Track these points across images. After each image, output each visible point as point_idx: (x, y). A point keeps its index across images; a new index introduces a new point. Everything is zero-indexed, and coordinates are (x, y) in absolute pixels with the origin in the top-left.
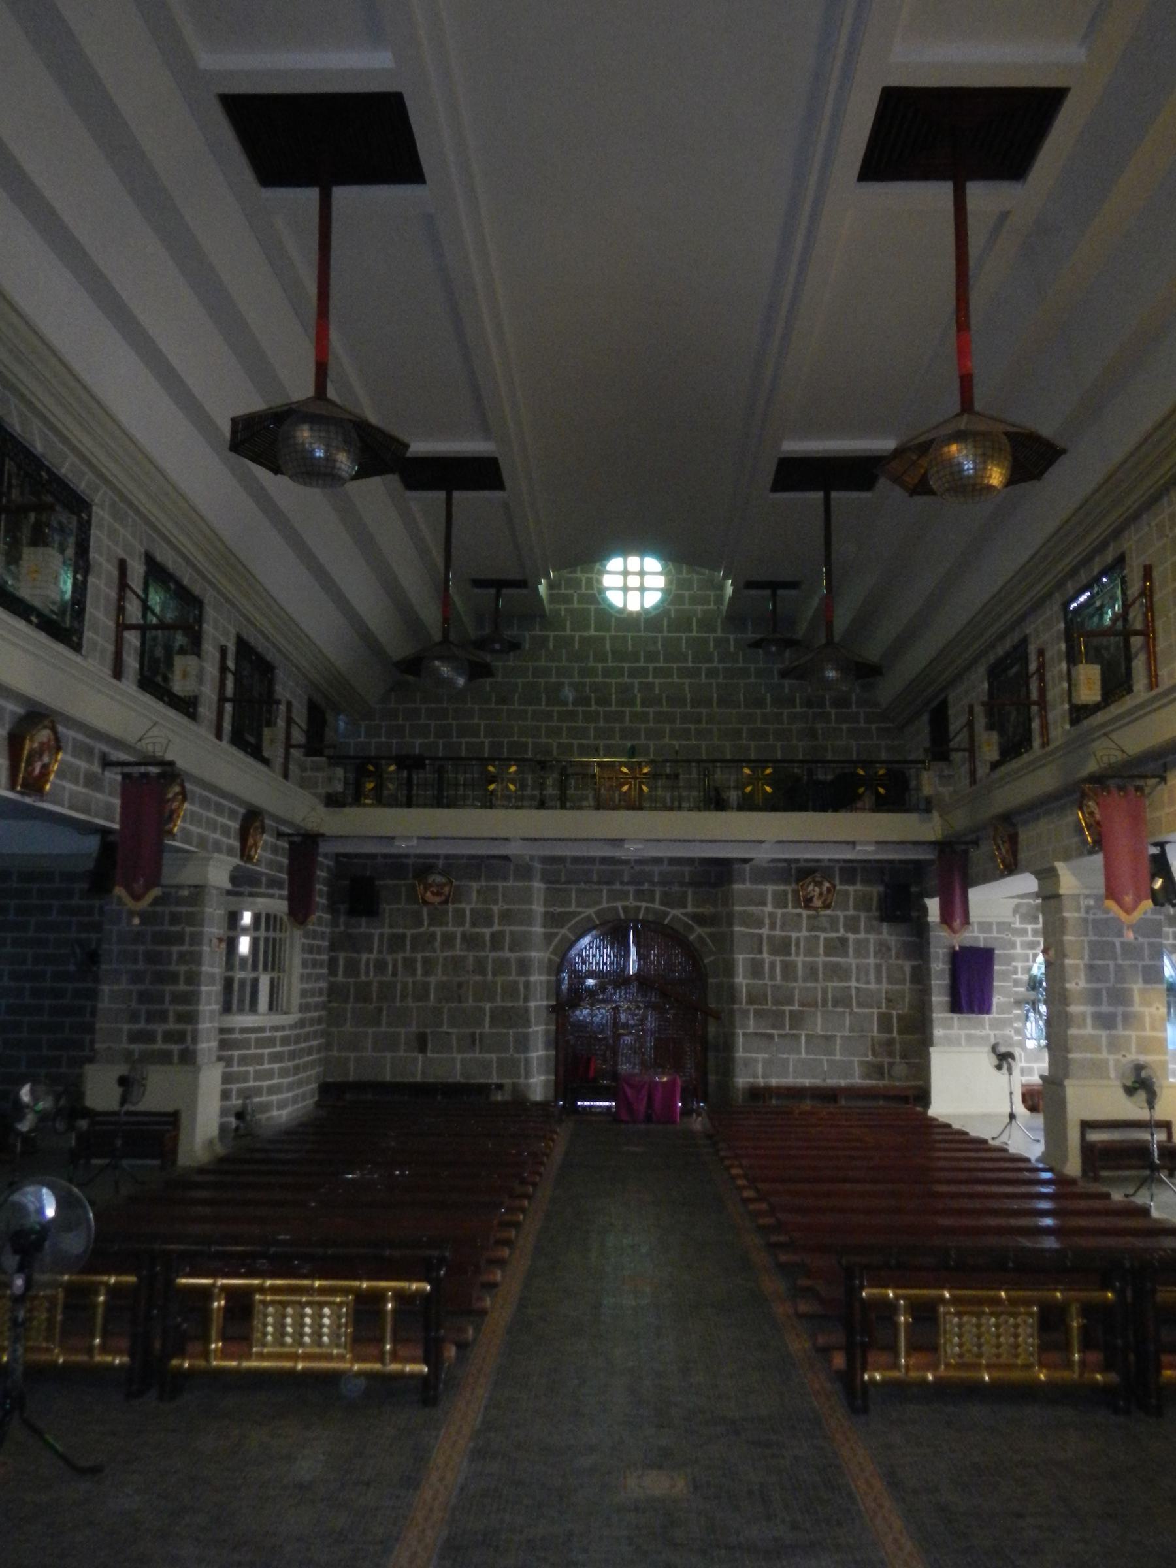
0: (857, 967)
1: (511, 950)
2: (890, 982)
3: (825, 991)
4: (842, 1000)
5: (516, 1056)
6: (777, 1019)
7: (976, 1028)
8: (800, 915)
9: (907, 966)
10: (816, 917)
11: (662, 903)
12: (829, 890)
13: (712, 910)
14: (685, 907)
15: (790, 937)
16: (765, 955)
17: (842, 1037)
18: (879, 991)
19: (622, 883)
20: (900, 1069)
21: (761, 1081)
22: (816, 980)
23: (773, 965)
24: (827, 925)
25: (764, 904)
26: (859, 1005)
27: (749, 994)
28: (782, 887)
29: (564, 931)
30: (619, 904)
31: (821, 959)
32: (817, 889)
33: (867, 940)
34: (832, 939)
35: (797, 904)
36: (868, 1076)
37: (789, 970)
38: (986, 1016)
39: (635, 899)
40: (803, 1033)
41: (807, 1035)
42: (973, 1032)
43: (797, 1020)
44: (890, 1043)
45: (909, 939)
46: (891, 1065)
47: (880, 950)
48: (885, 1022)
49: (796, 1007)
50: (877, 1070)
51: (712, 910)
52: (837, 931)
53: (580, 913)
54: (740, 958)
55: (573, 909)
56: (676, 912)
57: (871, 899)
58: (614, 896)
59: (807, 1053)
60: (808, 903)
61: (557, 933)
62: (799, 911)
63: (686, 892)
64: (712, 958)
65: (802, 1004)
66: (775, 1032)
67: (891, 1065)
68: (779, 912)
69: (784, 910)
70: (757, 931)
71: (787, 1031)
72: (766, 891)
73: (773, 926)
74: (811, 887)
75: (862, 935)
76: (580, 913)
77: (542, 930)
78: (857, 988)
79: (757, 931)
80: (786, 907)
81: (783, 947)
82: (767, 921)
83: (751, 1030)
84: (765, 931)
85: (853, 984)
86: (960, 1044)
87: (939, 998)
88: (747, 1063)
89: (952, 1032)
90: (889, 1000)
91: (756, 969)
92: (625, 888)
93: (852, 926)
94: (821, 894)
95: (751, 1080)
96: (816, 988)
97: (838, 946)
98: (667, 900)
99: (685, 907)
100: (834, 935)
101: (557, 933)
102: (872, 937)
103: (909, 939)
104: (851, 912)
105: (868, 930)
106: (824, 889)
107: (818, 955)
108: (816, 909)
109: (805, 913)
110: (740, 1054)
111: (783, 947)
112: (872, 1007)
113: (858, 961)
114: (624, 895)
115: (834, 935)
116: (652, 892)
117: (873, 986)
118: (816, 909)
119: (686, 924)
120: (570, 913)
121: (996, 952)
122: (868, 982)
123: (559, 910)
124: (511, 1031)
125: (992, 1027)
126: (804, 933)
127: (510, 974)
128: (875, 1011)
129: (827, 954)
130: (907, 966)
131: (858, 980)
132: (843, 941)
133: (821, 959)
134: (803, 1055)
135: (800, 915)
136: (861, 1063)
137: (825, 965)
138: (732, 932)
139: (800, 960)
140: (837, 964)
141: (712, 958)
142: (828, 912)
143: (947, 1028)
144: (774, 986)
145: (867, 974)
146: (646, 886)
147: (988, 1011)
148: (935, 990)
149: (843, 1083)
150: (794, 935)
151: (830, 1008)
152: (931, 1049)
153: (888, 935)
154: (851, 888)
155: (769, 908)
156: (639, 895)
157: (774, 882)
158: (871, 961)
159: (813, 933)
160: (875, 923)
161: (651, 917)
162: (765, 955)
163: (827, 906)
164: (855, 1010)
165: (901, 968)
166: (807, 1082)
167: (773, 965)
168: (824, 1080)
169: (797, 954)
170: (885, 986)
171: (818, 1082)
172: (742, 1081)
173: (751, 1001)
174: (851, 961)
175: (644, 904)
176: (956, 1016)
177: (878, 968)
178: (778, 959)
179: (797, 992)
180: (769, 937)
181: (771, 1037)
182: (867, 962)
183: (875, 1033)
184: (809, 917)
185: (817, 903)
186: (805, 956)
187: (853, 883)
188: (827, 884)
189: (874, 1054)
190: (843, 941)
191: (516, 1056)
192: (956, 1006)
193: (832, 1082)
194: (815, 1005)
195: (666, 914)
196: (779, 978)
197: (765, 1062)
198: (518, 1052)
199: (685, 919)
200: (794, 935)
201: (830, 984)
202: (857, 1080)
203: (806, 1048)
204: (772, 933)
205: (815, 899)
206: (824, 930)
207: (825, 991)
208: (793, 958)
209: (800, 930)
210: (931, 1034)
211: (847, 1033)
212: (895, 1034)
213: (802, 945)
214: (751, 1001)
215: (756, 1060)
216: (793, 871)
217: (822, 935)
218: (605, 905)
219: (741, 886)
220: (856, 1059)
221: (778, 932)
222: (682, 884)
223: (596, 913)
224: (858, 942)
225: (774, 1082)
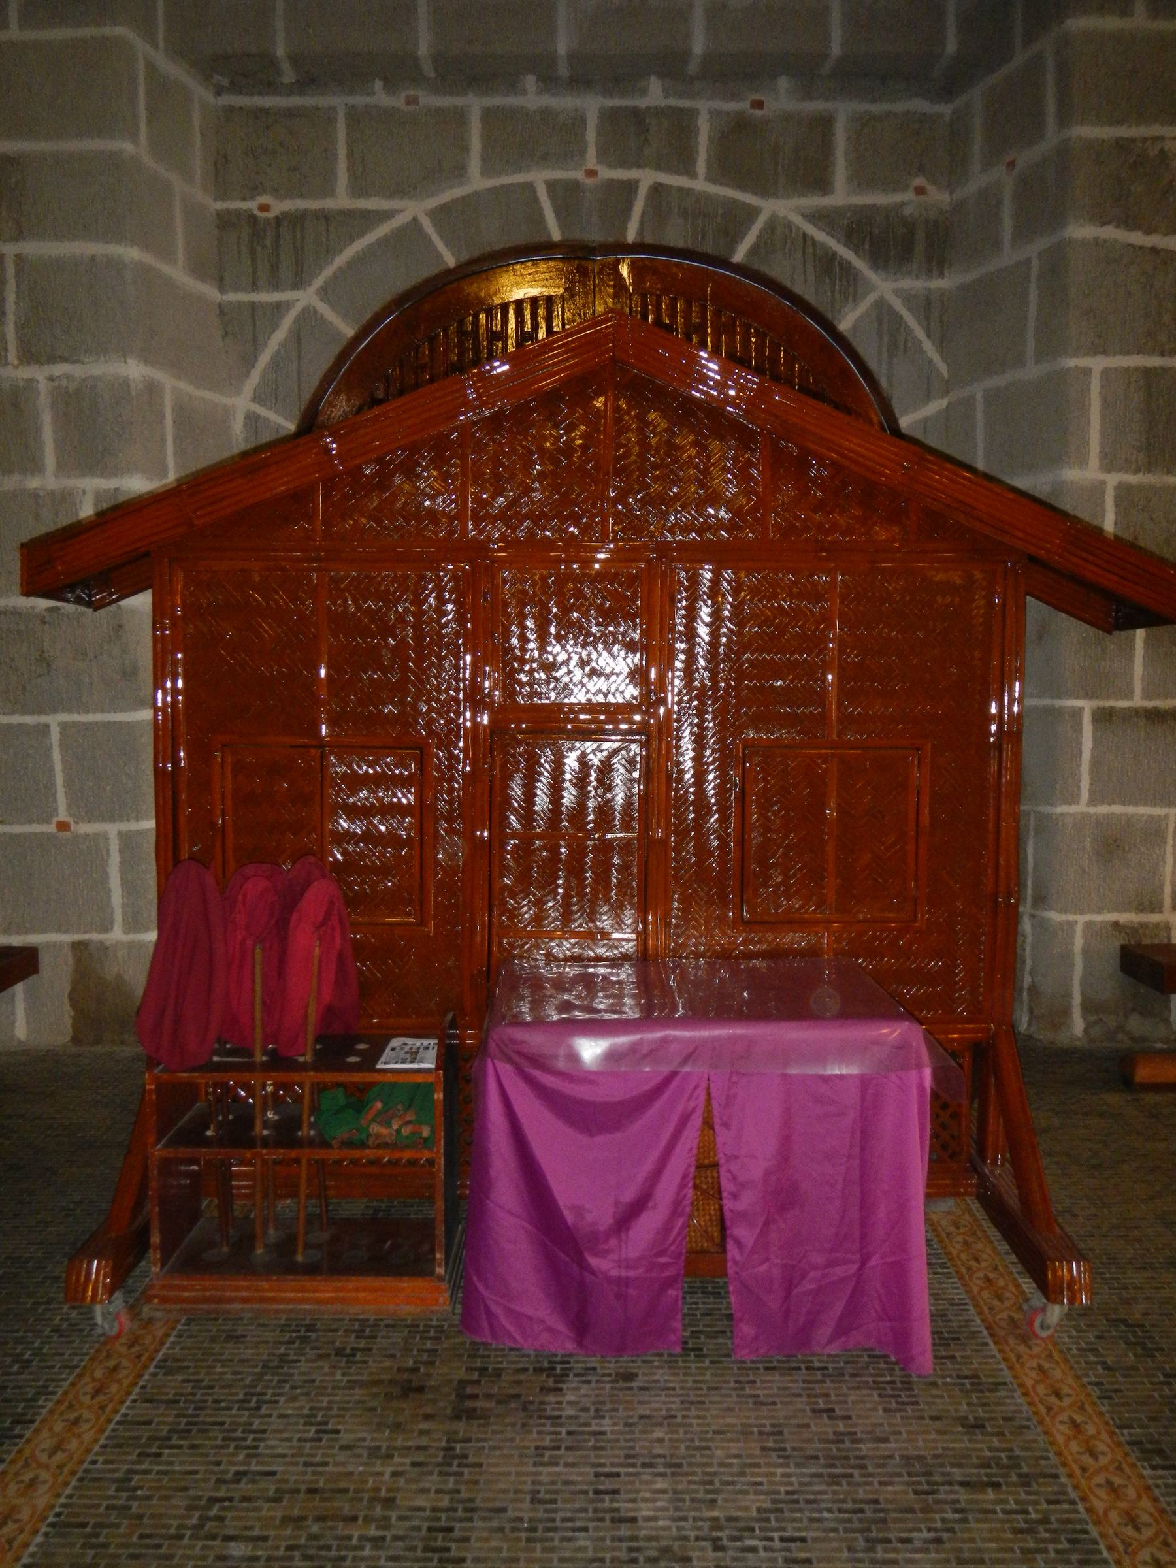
1: (29, 356)
5: (85, 828)
11: (727, 167)
13: (939, 197)
14: (822, 185)
19: (549, 82)
29: (305, 298)
30: (539, 177)
39: (603, 154)
51: (939, 197)
53: (370, 219)
55: (341, 200)
56: (786, 208)
58: (515, 139)
61: (279, 309)
63: (825, 123)
64: (936, 406)
76: (370, 219)
77: (210, 292)
83: (1138, 701)
92: (565, 103)
98: (745, 154)
99: (822, 185)
101: (279, 309)
114: (563, 137)
116: (681, 125)
119: (828, 264)
120: (325, 217)
123: (280, 206)
124: (54, 721)
127: (34, 465)
141: (936, 406)
146: (655, 94)
156: (628, 134)
161: (675, 235)
175: (646, 178)
191: (85, 828)
195: (736, 220)
198: (91, 815)
199: (821, 236)
218: (477, 181)
222: (806, 71)
223: (440, 215)
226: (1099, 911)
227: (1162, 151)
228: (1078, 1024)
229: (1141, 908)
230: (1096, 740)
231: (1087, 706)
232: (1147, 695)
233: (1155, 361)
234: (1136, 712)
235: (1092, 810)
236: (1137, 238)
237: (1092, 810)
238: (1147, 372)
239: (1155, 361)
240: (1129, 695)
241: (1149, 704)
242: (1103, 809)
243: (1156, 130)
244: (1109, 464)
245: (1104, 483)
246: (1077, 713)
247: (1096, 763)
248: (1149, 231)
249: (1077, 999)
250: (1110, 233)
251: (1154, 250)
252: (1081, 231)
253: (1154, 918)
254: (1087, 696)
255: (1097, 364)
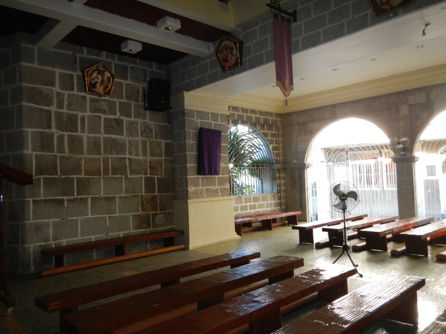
0: (130, 142)
2: (152, 155)
3: (106, 161)
4: (119, 169)
6: (66, 186)
7: (210, 184)
8: (84, 98)
9: (163, 143)
10: (97, 101)
12: (108, 78)
15: (76, 115)
16: (54, 130)
17: (120, 197)
18: (146, 161)
20: (160, 218)
21: (53, 243)
22: (99, 154)
23: (61, 138)
24: (105, 107)
25: (53, 84)
26: (132, 172)
27: (39, 166)
28: (69, 72)
31: (102, 136)
32: (99, 76)
33: (137, 122)
34: (110, 119)
35: (82, 88)
36: (139, 227)
37: (75, 144)
38: (216, 176)
40: (90, 197)
41: (92, 198)
42: (209, 187)
43: (83, 186)
44: (153, 199)
45: (163, 124)
46: (154, 216)
47: (145, 131)
48: (149, 183)
49: (83, 176)
50: (144, 221)
52: (115, 114)
54: (30, 132)
57: (138, 92)
59: (92, 215)
60: (92, 88)
62: (83, 94)
65: (87, 173)
66: (65, 198)
67: (154, 216)
68: (66, 93)
69: (71, 92)
70: (46, 108)
71: (76, 197)
72: (54, 73)
73: (60, 105)
74: (95, 74)
75: (133, 119)
78: (128, 158)
79: (46, 108)
80: (72, 89)
81: (69, 123)
82: (55, 100)
83: (42, 198)
84: (53, 108)
85: (127, 156)
86: (203, 197)
87: (191, 165)
88: (38, 228)
89: (198, 188)
90: (152, 168)
91: (45, 142)
93: (126, 112)
94: (103, 81)
95: (43, 243)
96: (99, 159)
97: (115, 126)
100: (113, 117)
102: (140, 121)
103: (163, 124)
104: (124, 100)
105: (137, 115)
106: (106, 77)
107: (100, 133)
108: (99, 95)
109: (89, 96)
110: (31, 221)
111: (69, 123)
112: (141, 175)
113: (131, 138)
115: (113, 117)
117: (141, 158)
118: (99, 95)
121: (222, 134)
122: (137, 155)
125: (220, 184)
126: (88, 113)
128: (143, 176)
129: (106, 133)
130: (163, 143)
131: (130, 153)
132: (119, 122)
133: (102, 136)
134: (90, 216)
135: (84, 98)
136: (134, 216)
137: (106, 140)
138: (20, 109)
139: (85, 136)
140: (114, 140)
142: (107, 98)
143: (196, 184)
144: (63, 157)
145: (137, 149)
147: (216, 173)
148: (188, 159)
149: (121, 234)
150: (80, 114)
151: (110, 175)
152: (189, 201)
153: (151, 120)
154: (124, 82)
155: (57, 89)
157: (61, 67)
158: (140, 139)
159: (96, 114)
160: (142, 111)
162: (54, 130)
163: (108, 93)
164: (129, 176)
165: (159, 144)
166: (93, 238)
167: (61, 138)
168: (107, 234)
169: (83, 131)
170: (149, 157)
171: (101, 236)
172: (33, 246)
173: (40, 171)
174: (125, 138)
176: (200, 177)
177: (144, 143)
178: (66, 133)
179: (83, 162)
180: (56, 113)
181: (61, 202)
182: (138, 139)
183: (144, 194)
184: (91, 100)
185: (100, 89)
186: (89, 132)
187: (126, 78)
188: (107, 74)
189: (143, 210)
190: (119, 122)
192: (201, 171)
193: (113, 234)
194: (99, 173)
196: (67, 150)
197: (55, 224)
200: (80, 114)
201: (110, 156)
202: (132, 231)
203: (92, 208)
204: (61, 111)
205: (98, 84)
206: (104, 112)
207: (106, 161)
208: (79, 133)
209: (85, 111)
210: (187, 191)
211: (124, 195)
212: (156, 193)
213: (86, 122)
214: (40, 171)
215: (47, 225)
216: (78, 60)
217: (103, 116)
219: (30, 65)
220: (131, 214)
221: (65, 111)
224: (130, 124)
225: (64, 242)
226: (36, 243)
227: (42, 90)
228: (32, 268)
229: (45, 241)
230: (34, 207)
231: (31, 200)
232: (44, 196)
233: (42, 130)
234: (42, 200)
235: (33, 221)
236: (37, 106)
237: (33, 221)
238: (41, 132)
239: (42, 130)
240: (40, 197)
241: (45, 198)
242: (36, 221)
243: (40, 86)
244: (33, 150)
245: (32, 154)
246: (29, 201)
247: (33, 211)
248: (40, 105)
249: (32, 263)
250: (31, 104)
251: (41, 109)
252: (25, 104)
253: (49, 243)
254: (30, 198)
255: (30, 130)
